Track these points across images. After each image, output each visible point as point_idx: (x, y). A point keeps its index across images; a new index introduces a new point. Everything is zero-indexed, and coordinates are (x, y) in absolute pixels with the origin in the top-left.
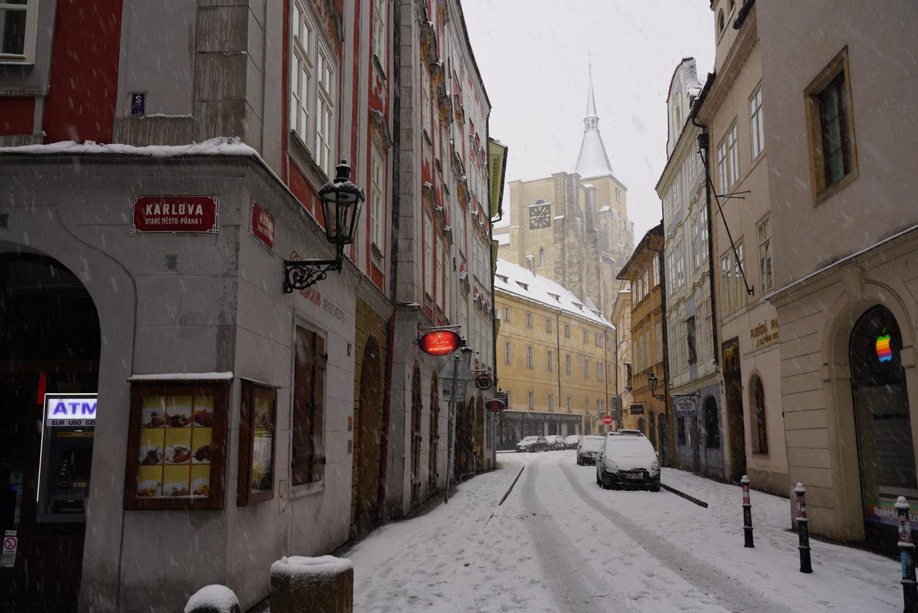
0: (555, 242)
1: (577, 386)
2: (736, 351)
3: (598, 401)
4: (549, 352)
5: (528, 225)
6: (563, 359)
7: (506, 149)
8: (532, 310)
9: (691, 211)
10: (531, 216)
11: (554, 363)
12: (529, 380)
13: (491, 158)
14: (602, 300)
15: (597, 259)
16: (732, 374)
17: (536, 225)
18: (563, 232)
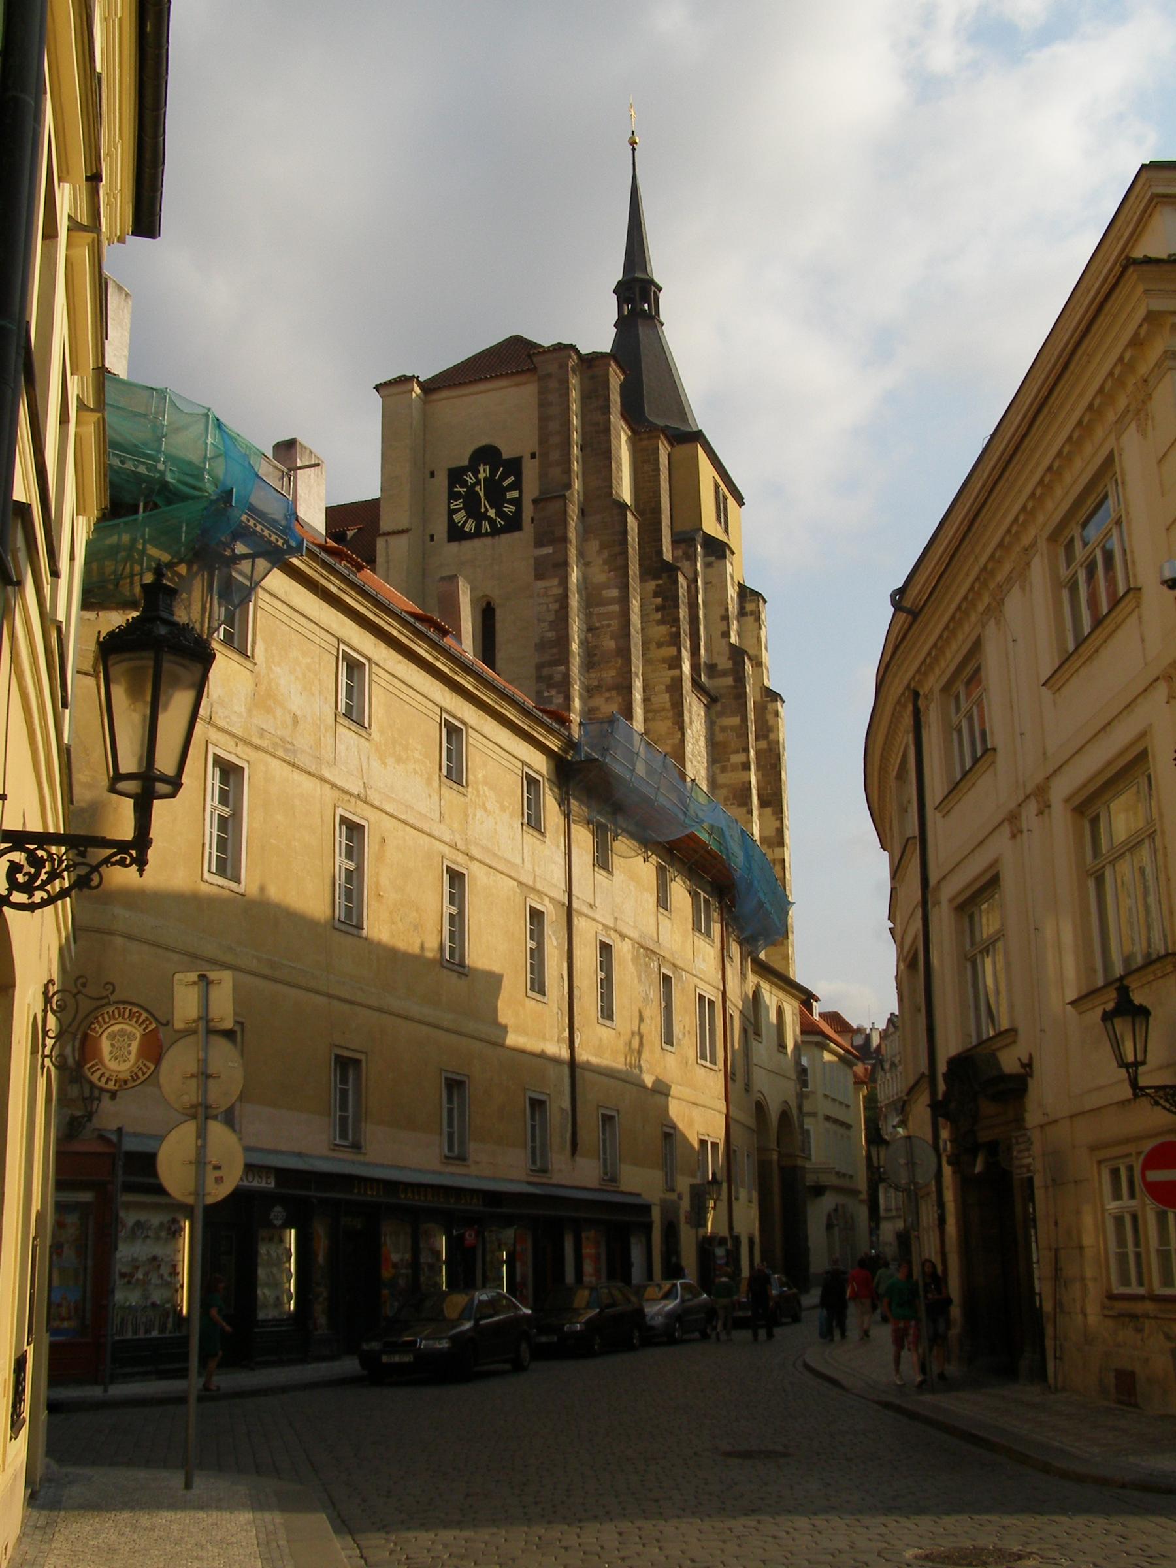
0: (539, 576)
4: (536, 916)
5: (440, 528)
15: (676, 663)
17: (470, 526)
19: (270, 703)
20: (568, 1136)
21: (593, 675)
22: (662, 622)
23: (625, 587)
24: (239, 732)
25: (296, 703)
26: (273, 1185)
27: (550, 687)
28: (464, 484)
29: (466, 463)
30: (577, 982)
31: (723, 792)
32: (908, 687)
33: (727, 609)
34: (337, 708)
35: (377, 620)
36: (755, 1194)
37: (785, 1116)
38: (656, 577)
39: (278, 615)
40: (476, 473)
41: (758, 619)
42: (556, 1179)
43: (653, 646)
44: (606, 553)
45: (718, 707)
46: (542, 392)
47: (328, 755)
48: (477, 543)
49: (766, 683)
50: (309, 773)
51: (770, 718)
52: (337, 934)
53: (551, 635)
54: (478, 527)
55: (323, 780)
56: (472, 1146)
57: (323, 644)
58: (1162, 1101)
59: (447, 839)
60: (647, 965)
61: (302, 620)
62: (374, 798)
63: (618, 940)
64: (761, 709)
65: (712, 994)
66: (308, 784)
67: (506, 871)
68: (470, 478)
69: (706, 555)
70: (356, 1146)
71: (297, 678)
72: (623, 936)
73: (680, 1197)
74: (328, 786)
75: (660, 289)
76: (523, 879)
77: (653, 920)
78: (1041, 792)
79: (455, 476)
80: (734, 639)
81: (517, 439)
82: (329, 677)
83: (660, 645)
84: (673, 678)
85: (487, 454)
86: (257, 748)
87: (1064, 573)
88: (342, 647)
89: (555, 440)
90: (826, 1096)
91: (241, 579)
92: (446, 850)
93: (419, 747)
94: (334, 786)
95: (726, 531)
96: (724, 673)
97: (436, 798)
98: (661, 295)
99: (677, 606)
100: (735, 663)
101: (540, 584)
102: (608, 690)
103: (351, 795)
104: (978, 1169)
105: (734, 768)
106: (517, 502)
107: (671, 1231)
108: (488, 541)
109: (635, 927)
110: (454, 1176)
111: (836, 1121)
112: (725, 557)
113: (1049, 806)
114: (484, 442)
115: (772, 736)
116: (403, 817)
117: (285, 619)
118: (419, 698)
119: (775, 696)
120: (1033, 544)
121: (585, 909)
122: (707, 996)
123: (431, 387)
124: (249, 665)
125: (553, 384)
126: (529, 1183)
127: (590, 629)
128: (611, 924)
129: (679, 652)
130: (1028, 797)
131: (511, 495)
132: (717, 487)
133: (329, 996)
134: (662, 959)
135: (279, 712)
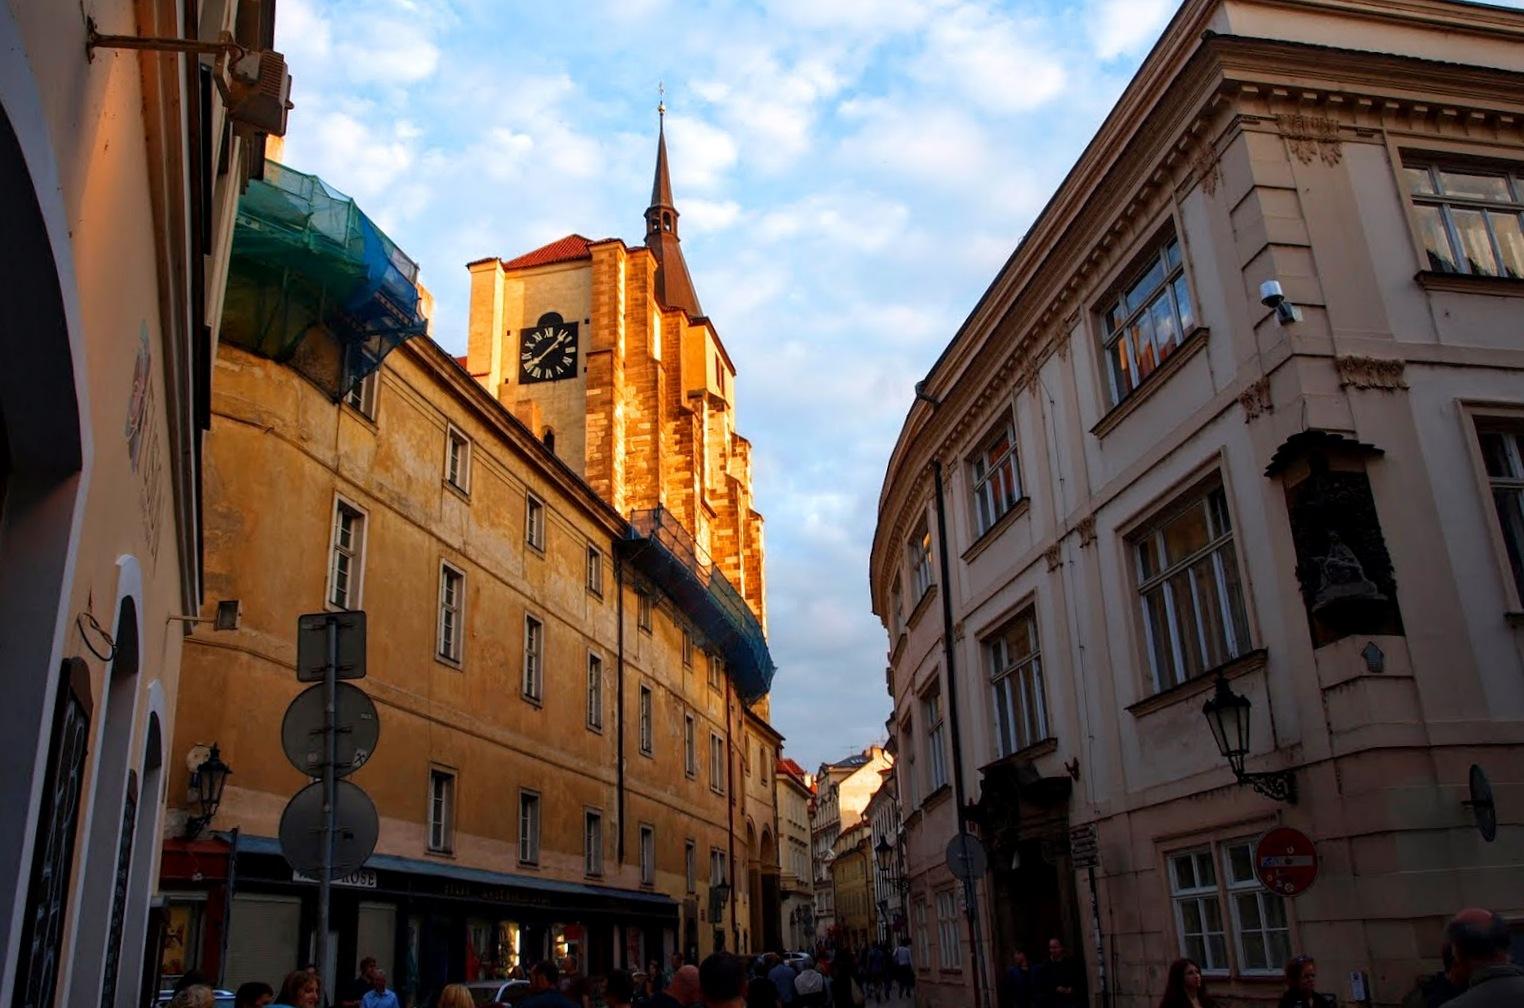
1: (667, 797)
3: (714, 854)
6: (632, 697)
8: (546, 492)
11: (609, 705)
12: (524, 743)
15: (689, 483)
17: (537, 373)
18: (612, 384)
19: (389, 463)
20: (617, 847)
21: (629, 488)
22: (680, 453)
23: (655, 422)
24: (361, 484)
25: (411, 464)
26: (375, 886)
28: (533, 341)
29: (534, 325)
30: (625, 718)
32: (931, 461)
33: (724, 449)
34: (444, 474)
35: (479, 407)
36: (747, 897)
37: (766, 835)
38: (676, 418)
39: (398, 390)
40: (543, 334)
41: (745, 459)
42: (607, 883)
43: (673, 470)
44: (641, 396)
45: (717, 521)
47: (436, 514)
48: (542, 386)
49: (752, 507)
50: (419, 527)
51: (753, 533)
52: (437, 665)
53: (598, 456)
54: (543, 373)
55: (431, 534)
56: (542, 853)
57: (437, 422)
58: (1264, 788)
59: (529, 594)
60: (676, 708)
61: (418, 399)
62: (471, 552)
63: (655, 687)
64: (748, 525)
65: (720, 735)
66: (418, 536)
67: (573, 623)
68: (538, 337)
69: (710, 408)
70: (448, 852)
71: (412, 446)
72: (659, 684)
73: (698, 898)
74: (434, 540)
75: (678, 215)
76: (586, 631)
77: (680, 672)
78: (1086, 529)
80: (728, 472)
82: (440, 446)
83: (678, 470)
84: (687, 496)
85: (551, 320)
86: (377, 500)
87: (1106, 337)
88: (450, 426)
89: (604, 309)
90: (790, 821)
91: (369, 355)
92: (528, 603)
93: (508, 516)
94: (439, 539)
95: (723, 392)
96: (721, 497)
97: (520, 559)
98: (679, 219)
99: (691, 441)
100: (730, 489)
101: (589, 418)
102: (640, 499)
103: (454, 549)
104: (1015, 865)
106: (574, 356)
107: (691, 926)
108: (550, 384)
109: (668, 678)
110: (525, 879)
111: (797, 841)
112: (723, 410)
113: (1096, 538)
114: (550, 310)
115: (754, 546)
116: (493, 571)
117: (403, 395)
118: (507, 473)
119: (755, 515)
120: (1076, 314)
121: (632, 661)
122: (717, 736)
123: (507, 268)
124: (373, 429)
125: (604, 268)
126: (587, 886)
127: (627, 453)
128: (650, 673)
129: (693, 475)
130: (1070, 533)
131: (569, 350)
133: (429, 718)
134: (686, 705)
135: (395, 471)
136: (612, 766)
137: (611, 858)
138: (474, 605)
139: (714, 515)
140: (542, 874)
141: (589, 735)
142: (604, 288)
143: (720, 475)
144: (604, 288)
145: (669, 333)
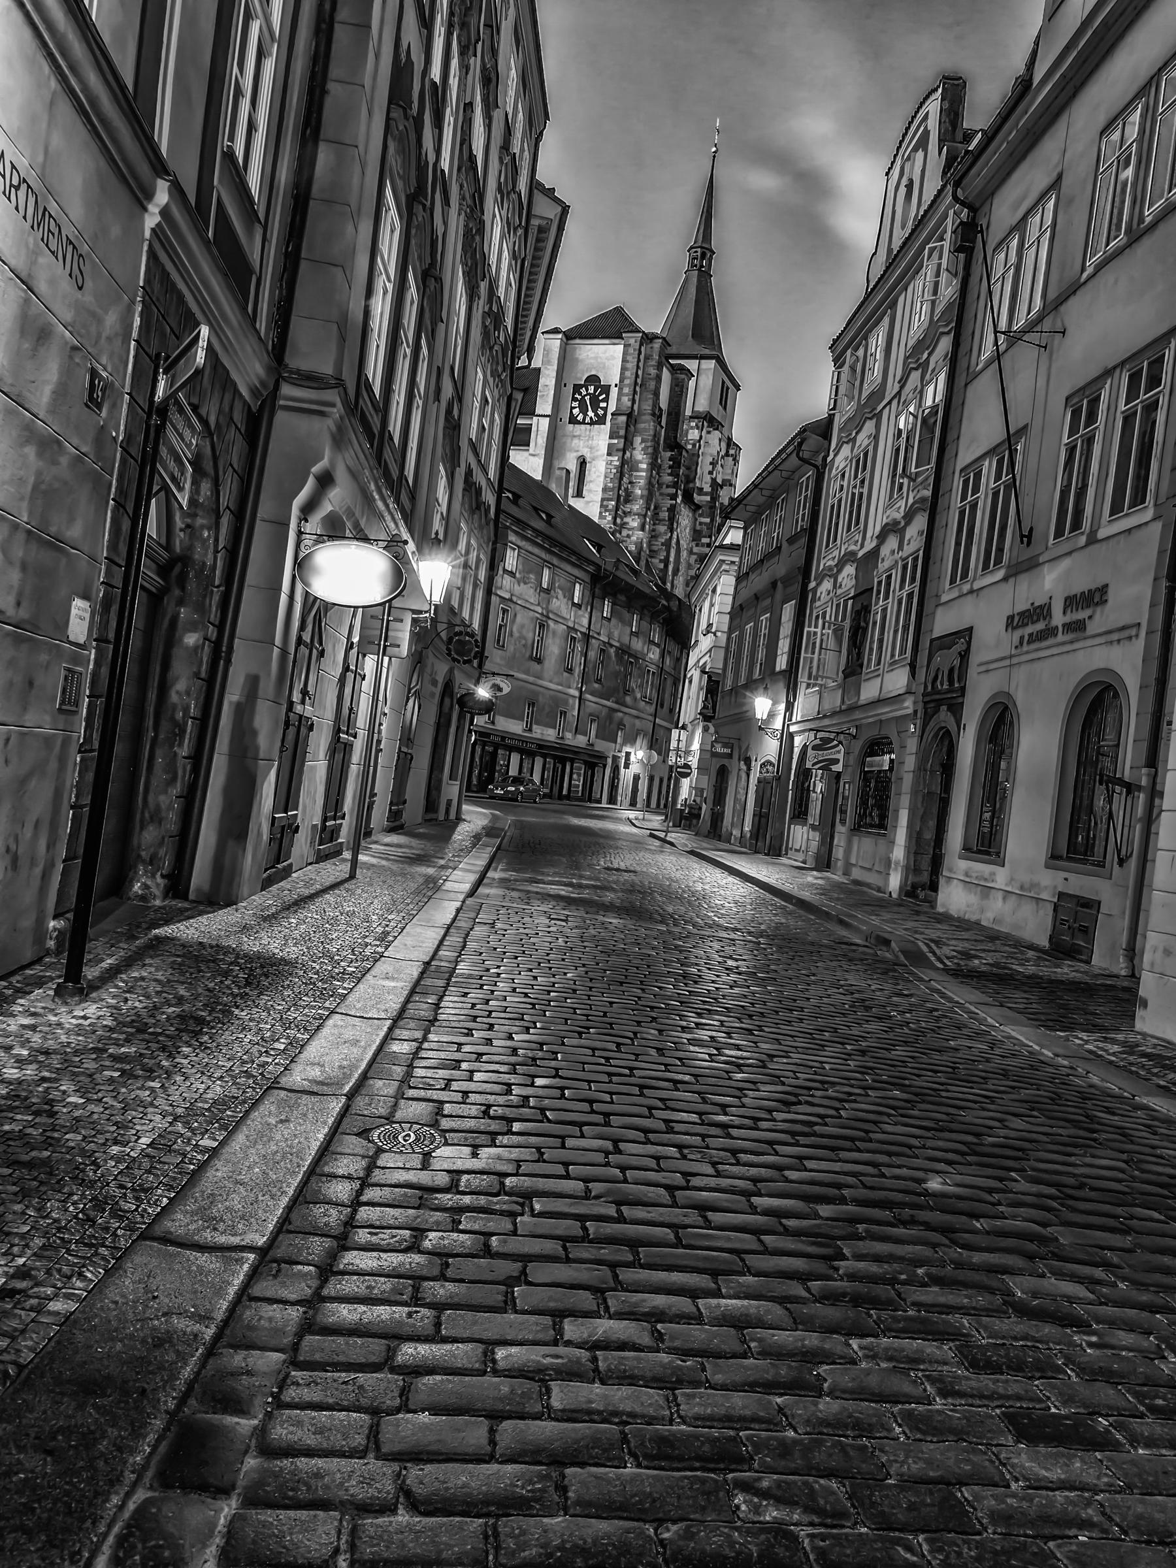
0: (609, 454)
2: (965, 656)
7: (565, 209)
9: (902, 388)
10: (574, 399)
13: (535, 222)
14: (671, 568)
15: (674, 497)
16: (941, 697)
17: (580, 418)
22: (669, 475)
27: (606, 511)
28: (580, 394)
31: (695, 557)
46: (625, 353)
53: (610, 485)
54: (584, 419)
56: (534, 727)
70: (493, 723)
79: (577, 388)
81: (612, 375)
83: (668, 487)
85: (593, 379)
89: (627, 382)
96: (706, 494)
101: (610, 458)
105: (703, 545)
114: (593, 373)
132: (723, 382)
136: (577, 688)
137: (570, 731)
138: (513, 621)
139: (698, 507)
140: (534, 735)
141: (565, 674)
142: (629, 365)
143: (708, 478)
144: (629, 365)
145: (677, 385)
